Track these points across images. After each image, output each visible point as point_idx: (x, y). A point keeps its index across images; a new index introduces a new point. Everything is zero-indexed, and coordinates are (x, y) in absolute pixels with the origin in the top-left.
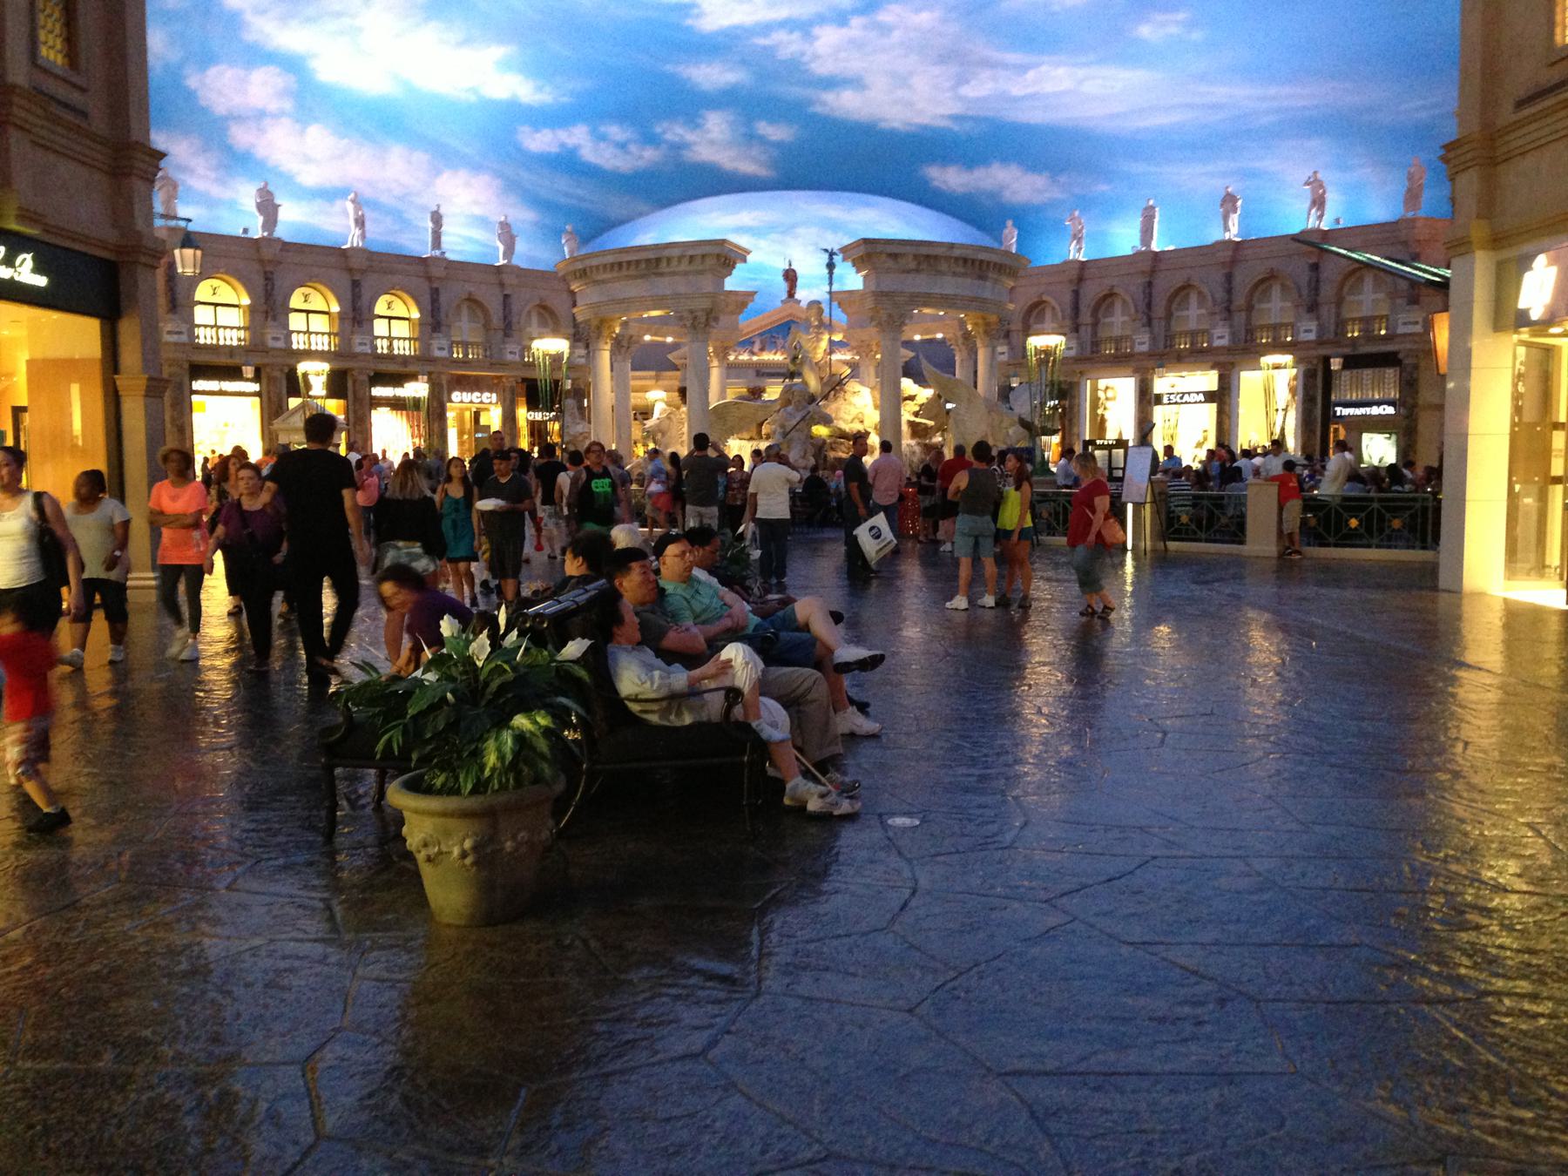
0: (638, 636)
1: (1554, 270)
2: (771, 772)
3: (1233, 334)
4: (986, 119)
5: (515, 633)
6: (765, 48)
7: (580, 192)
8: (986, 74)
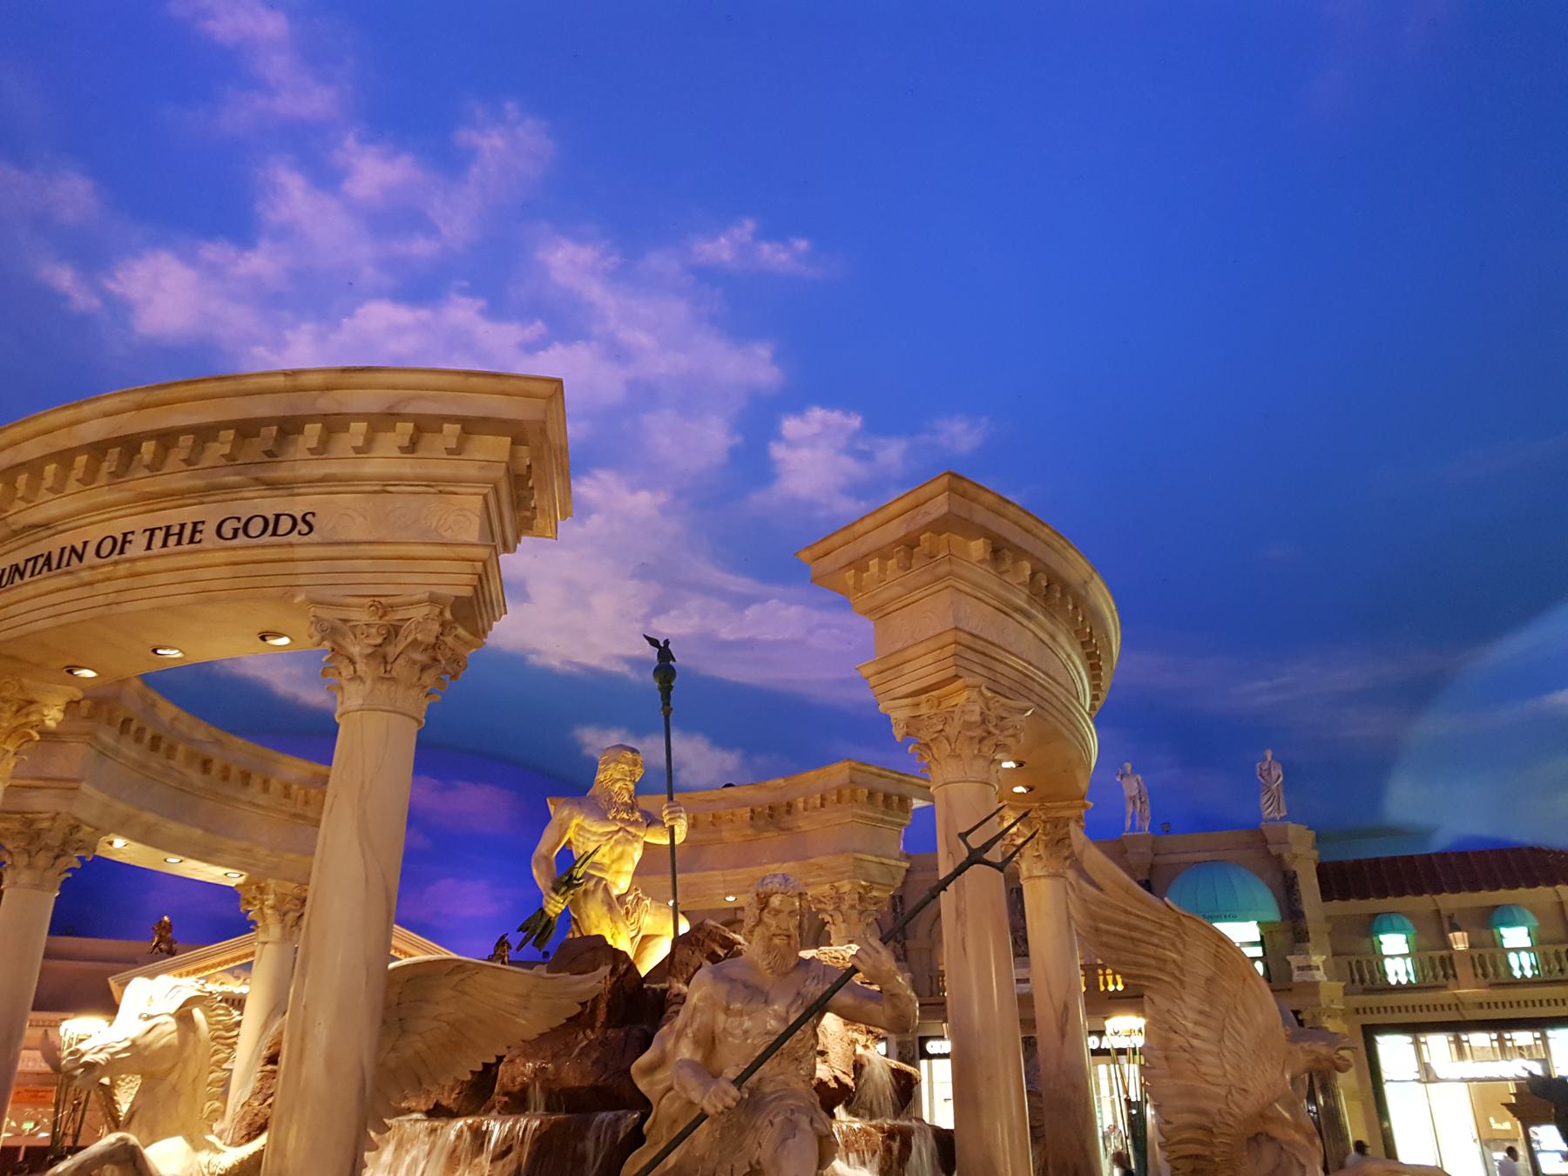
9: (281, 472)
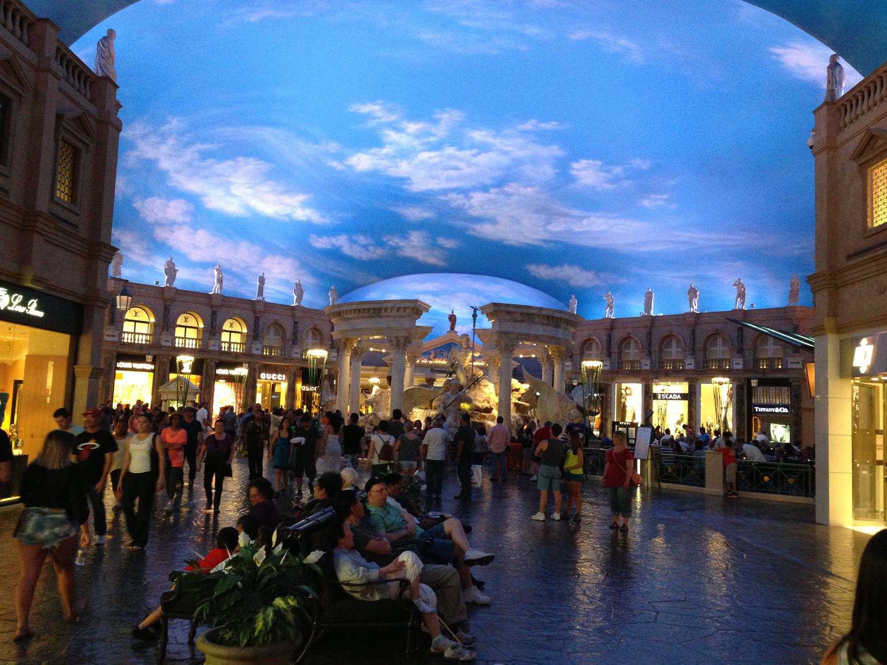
0: (352, 544)
1: (871, 347)
2: (424, 629)
3: (696, 363)
4: (561, 243)
5: (281, 545)
6: (445, 201)
7: (341, 269)
8: (562, 220)
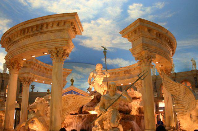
4: (117, 48)
9: (42, 31)
